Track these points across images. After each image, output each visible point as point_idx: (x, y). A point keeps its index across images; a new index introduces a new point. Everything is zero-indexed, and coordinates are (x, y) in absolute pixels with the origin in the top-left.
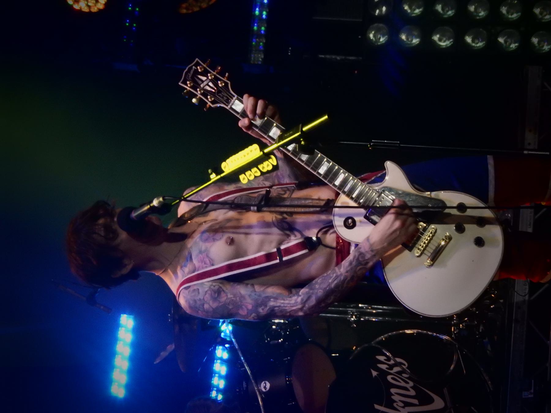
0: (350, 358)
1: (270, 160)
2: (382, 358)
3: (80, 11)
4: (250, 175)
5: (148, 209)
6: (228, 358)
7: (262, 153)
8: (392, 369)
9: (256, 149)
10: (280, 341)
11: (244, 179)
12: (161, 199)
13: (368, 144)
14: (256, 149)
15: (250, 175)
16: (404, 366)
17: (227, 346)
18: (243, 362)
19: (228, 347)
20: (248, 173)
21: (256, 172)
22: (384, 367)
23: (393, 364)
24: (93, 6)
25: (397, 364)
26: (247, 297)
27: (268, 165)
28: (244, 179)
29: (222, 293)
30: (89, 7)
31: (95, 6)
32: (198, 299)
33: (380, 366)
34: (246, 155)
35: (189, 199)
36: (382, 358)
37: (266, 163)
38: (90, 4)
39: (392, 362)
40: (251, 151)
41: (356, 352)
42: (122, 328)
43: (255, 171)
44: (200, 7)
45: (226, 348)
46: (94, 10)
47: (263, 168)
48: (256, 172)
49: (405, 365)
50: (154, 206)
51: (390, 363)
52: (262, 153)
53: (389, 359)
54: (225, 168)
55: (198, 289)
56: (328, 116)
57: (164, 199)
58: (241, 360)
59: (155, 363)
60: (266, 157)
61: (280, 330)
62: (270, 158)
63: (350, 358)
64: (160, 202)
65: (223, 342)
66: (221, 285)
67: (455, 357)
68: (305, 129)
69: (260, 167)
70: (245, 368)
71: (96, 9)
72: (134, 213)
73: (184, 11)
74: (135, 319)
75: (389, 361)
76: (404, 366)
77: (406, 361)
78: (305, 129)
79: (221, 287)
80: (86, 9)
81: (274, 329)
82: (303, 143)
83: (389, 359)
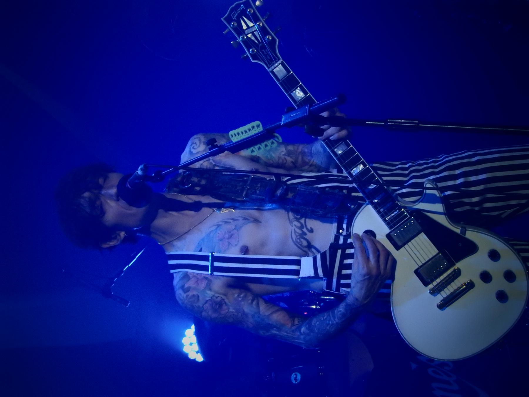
26: (250, 316)
29: (224, 305)
32: (197, 305)
55: (198, 296)
66: (224, 297)
79: (224, 300)
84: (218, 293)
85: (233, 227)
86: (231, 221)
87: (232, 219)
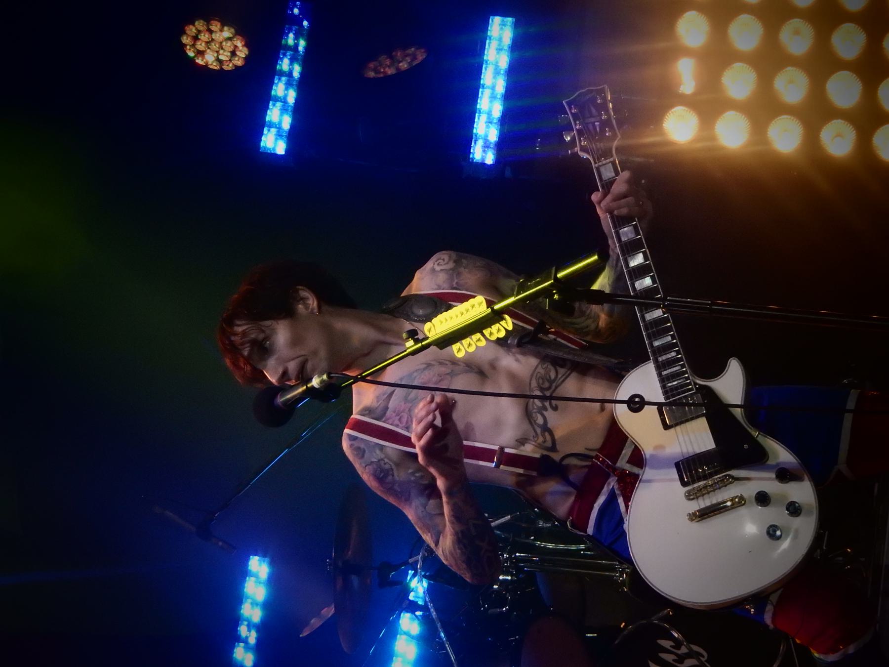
0: (616, 642)
1: (503, 323)
2: (666, 644)
3: (205, 67)
4: (470, 345)
5: (304, 392)
6: (420, 634)
7: (489, 310)
8: (681, 662)
9: (480, 304)
10: (504, 609)
11: (460, 350)
12: (325, 377)
13: (661, 302)
14: (480, 304)
15: (470, 345)
16: (702, 658)
17: (419, 613)
18: (443, 642)
19: (420, 616)
20: (466, 342)
21: (479, 340)
22: (669, 658)
23: (685, 654)
24: (226, 61)
25: (691, 655)
27: (499, 330)
28: (459, 350)
30: (220, 62)
31: (230, 60)
33: (664, 656)
34: (465, 312)
35: (368, 378)
36: (666, 644)
37: (495, 327)
38: (221, 57)
39: (684, 650)
40: (473, 306)
41: (626, 632)
42: (251, 578)
43: (478, 338)
44: (398, 69)
45: (416, 616)
46: (228, 67)
47: (491, 334)
48: (479, 340)
49: (703, 657)
50: (313, 387)
51: (679, 652)
52: (489, 310)
53: (678, 644)
54: (429, 331)
56: (598, 256)
57: (329, 377)
58: (440, 638)
59: (301, 636)
60: (495, 317)
61: (506, 593)
62: (503, 319)
63: (616, 642)
64: (322, 382)
65: (412, 607)
67: (782, 647)
68: (559, 275)
69: (486, 332)
70: (447, 650)
71: (231, 65)
72: (281, 398)
73: (372, 74)
74: (272, 563)
75: (679, 649)
76: (702, 658)
77: (704, 649)
78: (559, 275)
80: (215, 66)
81: (496, 590)
82: (556, 297)
83: (678, 644)
84: (389, 459)
85: (449, 371)
86: (447, 362)
87: (449, 361)
